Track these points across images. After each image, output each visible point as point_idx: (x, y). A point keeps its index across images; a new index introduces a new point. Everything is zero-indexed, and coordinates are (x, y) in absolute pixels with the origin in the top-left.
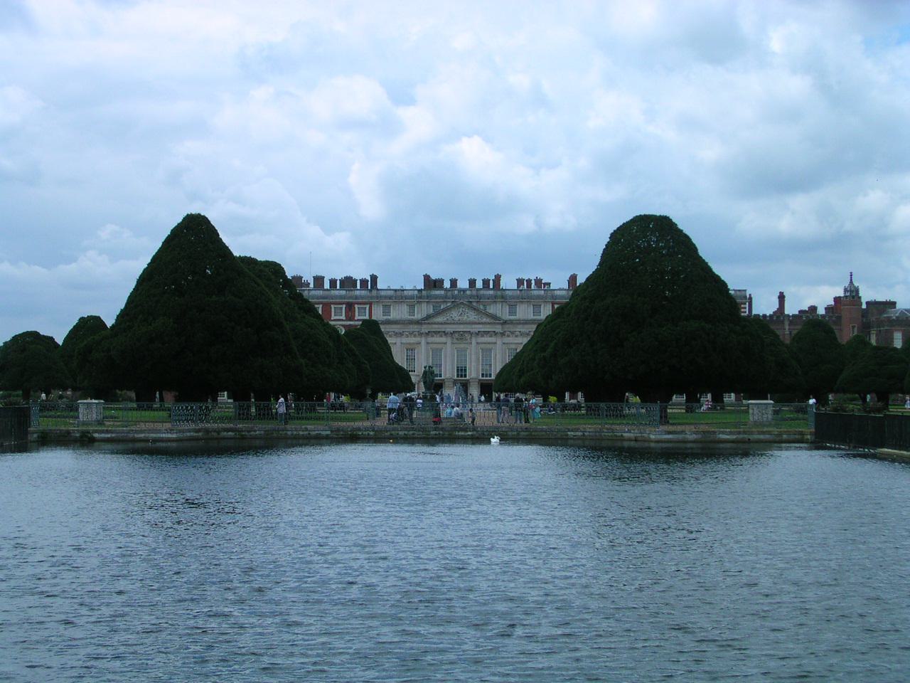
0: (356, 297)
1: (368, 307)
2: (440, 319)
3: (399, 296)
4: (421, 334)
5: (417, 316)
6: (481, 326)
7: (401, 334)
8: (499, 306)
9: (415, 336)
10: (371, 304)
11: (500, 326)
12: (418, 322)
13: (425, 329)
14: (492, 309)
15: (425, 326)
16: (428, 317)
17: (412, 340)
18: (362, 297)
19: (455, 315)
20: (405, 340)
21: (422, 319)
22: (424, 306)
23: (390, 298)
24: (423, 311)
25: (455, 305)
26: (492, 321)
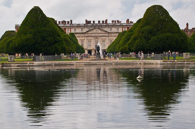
0: (67, 26)
1: (70, 29)
2: (90, 32)
3: (79, 26)
4: (85, 37)
5: (84, 31)
6: (102, 34)
7: (79, 37)
8: (107, 28)
9: (83, 37)
10: (71, 28)
11: (107, 34)
12: (84, 33)
13: (86, 35)
14: (105, 29)
15: (86, 34)
16: (87, 32)
17: (83, 38)
18: (68, 26)
19: (95, 31)
20: (80, 38)
21: (85, 32)
22: (86, 29)
23: (76, 26)
24: (85, 30)
25: (95, 28)
26: (105, 33)
